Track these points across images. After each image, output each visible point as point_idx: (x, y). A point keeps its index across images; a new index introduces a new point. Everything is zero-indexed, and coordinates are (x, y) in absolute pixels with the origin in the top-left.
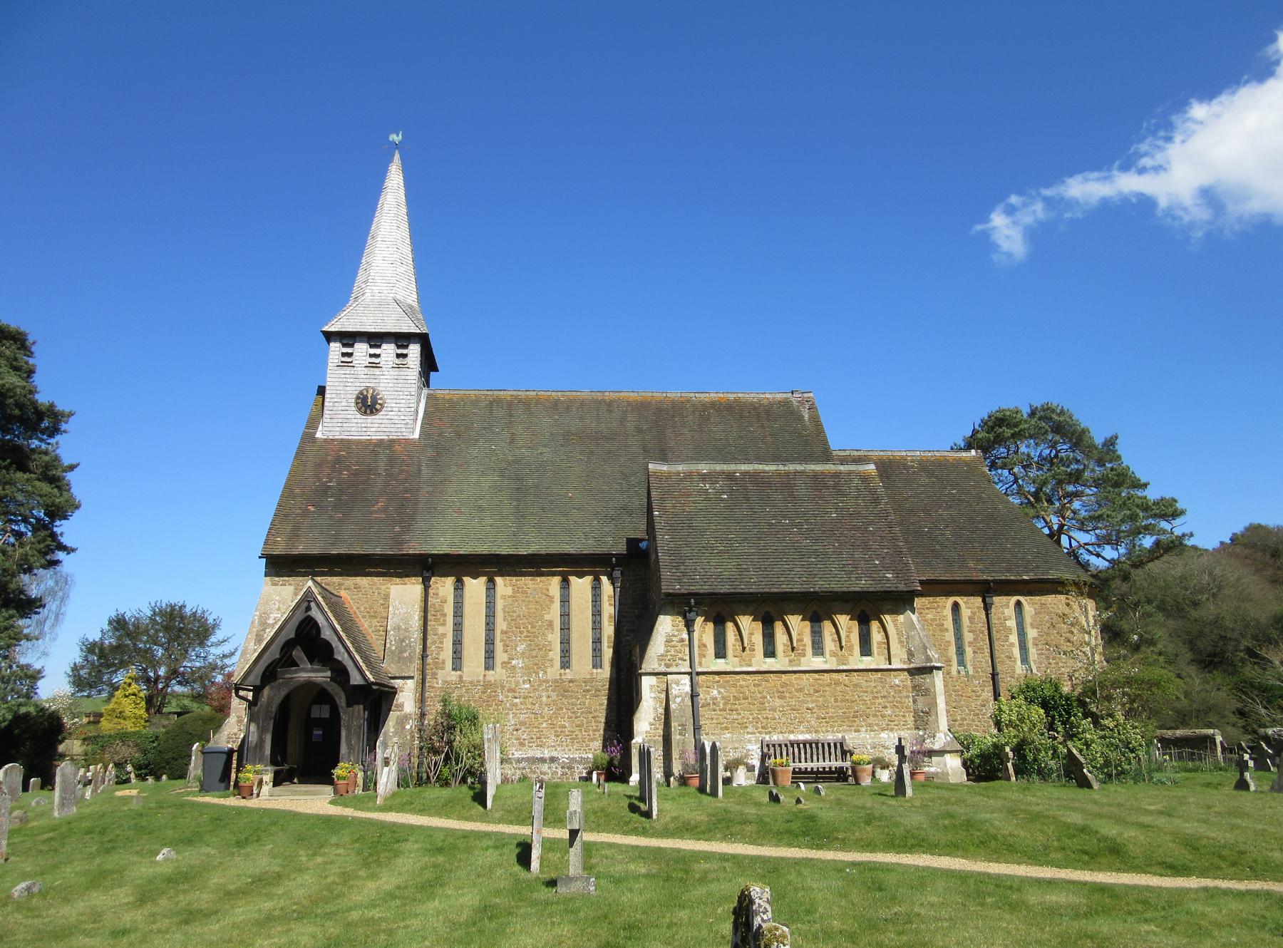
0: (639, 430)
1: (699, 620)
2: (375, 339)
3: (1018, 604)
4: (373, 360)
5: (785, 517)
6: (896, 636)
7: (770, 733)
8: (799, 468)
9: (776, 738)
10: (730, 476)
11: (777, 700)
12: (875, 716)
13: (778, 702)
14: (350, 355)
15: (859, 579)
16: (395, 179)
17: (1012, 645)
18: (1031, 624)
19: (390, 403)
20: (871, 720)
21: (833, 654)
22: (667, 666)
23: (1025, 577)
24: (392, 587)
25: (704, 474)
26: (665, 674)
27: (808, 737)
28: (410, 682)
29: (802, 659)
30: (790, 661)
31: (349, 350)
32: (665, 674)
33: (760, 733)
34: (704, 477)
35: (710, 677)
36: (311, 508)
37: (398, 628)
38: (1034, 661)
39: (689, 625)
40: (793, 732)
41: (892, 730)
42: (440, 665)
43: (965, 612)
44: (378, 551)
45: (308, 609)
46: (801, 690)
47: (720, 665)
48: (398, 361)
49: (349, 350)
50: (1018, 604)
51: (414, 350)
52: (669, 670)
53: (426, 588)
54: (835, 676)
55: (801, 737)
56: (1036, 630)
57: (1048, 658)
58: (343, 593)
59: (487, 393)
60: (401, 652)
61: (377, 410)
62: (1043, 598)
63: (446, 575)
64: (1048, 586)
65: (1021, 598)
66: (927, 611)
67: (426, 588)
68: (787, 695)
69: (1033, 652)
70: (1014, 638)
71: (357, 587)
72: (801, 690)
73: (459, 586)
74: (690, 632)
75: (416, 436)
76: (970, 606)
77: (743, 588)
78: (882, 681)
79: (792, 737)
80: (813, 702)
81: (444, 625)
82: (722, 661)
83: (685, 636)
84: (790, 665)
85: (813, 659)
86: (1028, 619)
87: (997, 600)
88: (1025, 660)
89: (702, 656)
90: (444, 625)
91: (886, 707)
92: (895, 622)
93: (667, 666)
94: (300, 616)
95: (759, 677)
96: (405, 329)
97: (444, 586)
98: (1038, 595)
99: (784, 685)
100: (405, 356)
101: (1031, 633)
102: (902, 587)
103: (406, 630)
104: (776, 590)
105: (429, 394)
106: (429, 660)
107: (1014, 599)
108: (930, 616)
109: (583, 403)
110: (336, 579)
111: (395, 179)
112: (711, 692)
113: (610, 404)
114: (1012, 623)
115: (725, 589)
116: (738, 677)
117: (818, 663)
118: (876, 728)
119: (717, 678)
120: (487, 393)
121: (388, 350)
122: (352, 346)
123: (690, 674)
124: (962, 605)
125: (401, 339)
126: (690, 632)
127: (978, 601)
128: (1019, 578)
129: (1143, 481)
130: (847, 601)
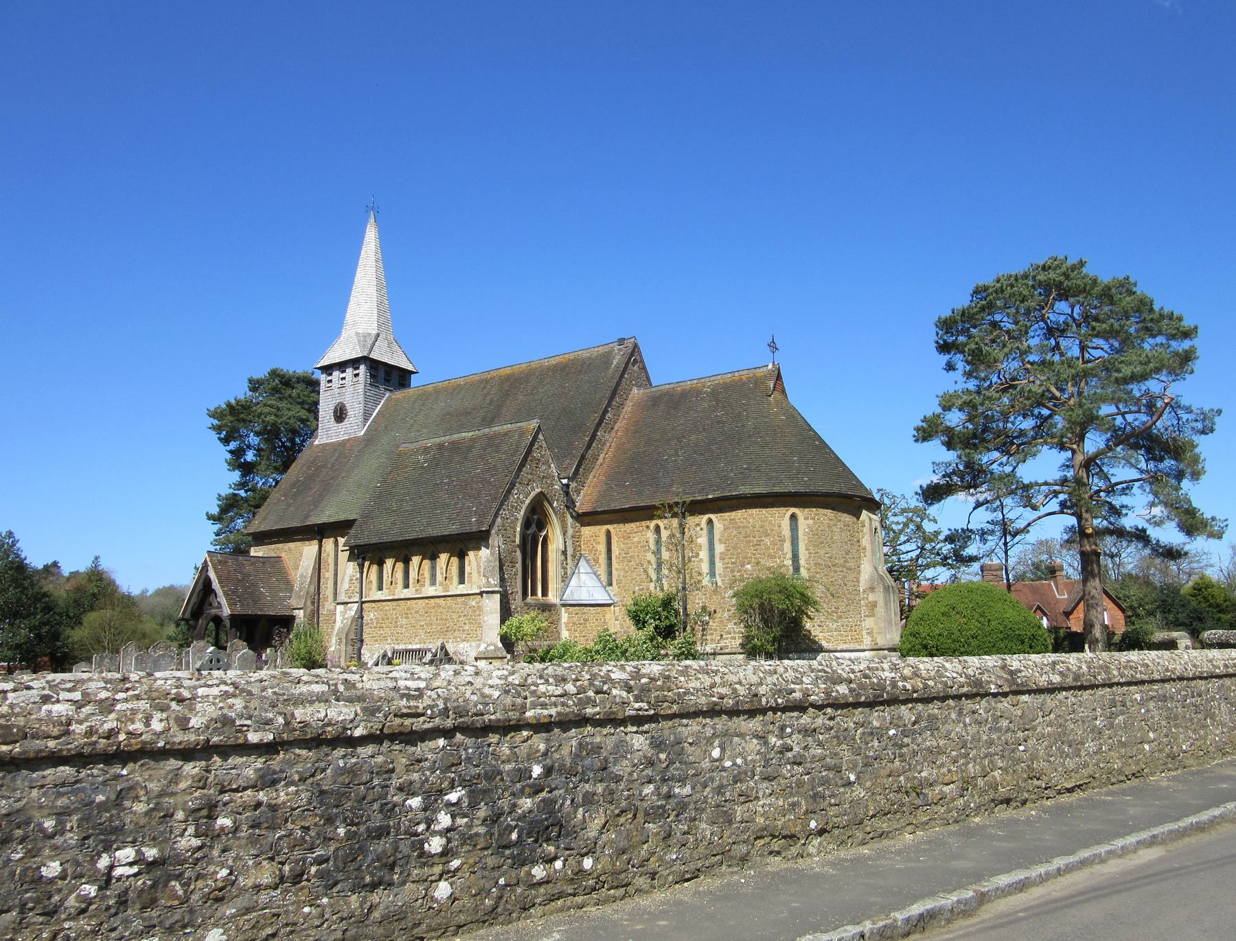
0: (492, 401)
1: (367, 564)
2: (342, 366)
3: (710, 522)
4: (343, 382)
5: (447, 477)
6: (476, 568)
7: (398, 644)
8: (487, 430)
9: (401, 647)
10: (441, 447)
11: (404, 619)
12: (459, 630)
13: (404, 621)
14: (330, 381)
15: (453, 524)
16: (371, 235)
17: (701, 560)
18: (720, 540)
19: (350, 413)
20: (456, 634)
21: (441, 584)
22: (350, 597)
23: (710, 497)
24: (305, 548)
25: (428, 447)
26: (347, 603)
27: (418, 646)
28: (302, 611)
29: (423, 589)
30: (416, 590)
31: (329, 378)
32: (347, 603)
33: (394, 643)
34: (426, 450)
35: (370, 604)
36: (283, 498)
37: (302, 576)
38: (720, 575)
39: (361, 567)
40: (410, 643)
41: (468, 641)
42: (326, 599)
43: (665, 534)
44: (294, 525)
45: (207, 571)
46: (416, 612)
47: (379, 595)
48: (355, 380)
49: (329, 378)
50: (710, 522)
51: (362, 368)
52: (349, 601)
53: (320, 547)
54: (437, 600)
55: (414, 647)
56: (723, 545)
57: (733, 571)
58: (283, 554)
59: (421, 388)
60: (301, 591)
61: (344, 419)
62: (733, 514)
63: (329, 537)
64: (734, 501)
65: (712, 516)
66: (634, 535)
67: (320, 547)
68: (410, 616)
69: (719, 565)
70: (704, 554)
71: (290, 550)
72: (416, 612)
73: (336, 543)
74: (362, 573)
75: (362, 433)
76: (668, 526)
77: (386, 539)
78: (465, 604)
79: (410, 647)
80: (424, 620)
81: (328, 571)
82: (380, 592)
83: (358, 576)
84: (417, 594)
85: (430, 588)
86: (717, 535)
87: (691, 520)
88: (712, 573)
89: (370, 589)
90: (328, 571)
91: (465, 624)
92: (476, 556)
93: (350, 597)
94: (203, 577)
95: (395, 603)
96: (354, 356)
97: (329, 544)
98: (728, 512)
99: (409, 609)
100: (356, 375)
101: (719, 548)
102: (474, 529)
103: (306, 577)
104: (400, 539)
105: (389, 397)
106: (321, 596)
107: (706, 517)
108: (636, 539)
109: (472, 385)
110: (280, 546)
111: (371, 235)
112: (369, 616)
113: (487, 381)
114: (703, 540)
115: (374, 540)
116: (384, 603)
117: (431, 591)
118: (459, 640)
119: (374, 605)
120: (421, 388)
121: (350, 371)
122: (330, 374)
123: (357, 602)
124: (662, 527)
125: (354, 363)
126: (362, 573)
127: (675, 522)
128: (705, 497)
129: (1187, 323)
130: (448, 542)
